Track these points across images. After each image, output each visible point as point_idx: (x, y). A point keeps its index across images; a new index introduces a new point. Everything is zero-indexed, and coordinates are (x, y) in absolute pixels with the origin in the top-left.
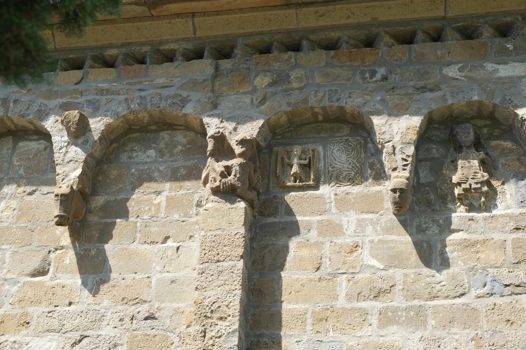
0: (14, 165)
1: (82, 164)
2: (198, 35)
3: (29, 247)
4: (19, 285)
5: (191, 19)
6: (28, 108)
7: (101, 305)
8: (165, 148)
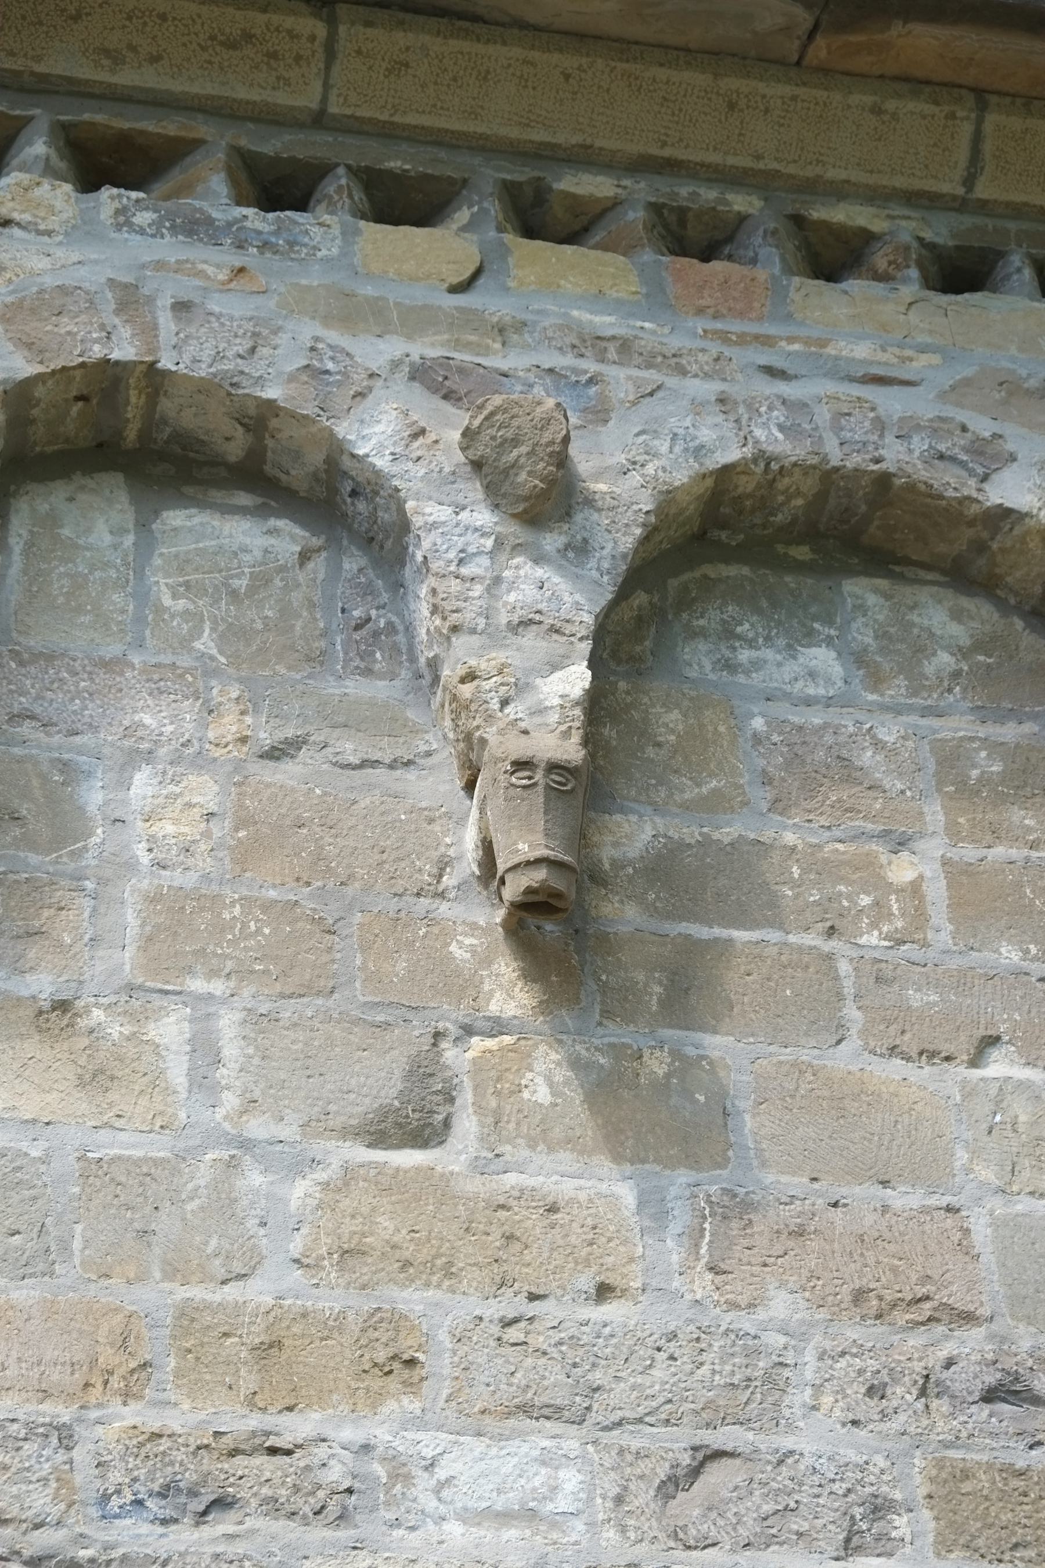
0: (159, 610)
1: (586, 647)
2: (983, 190)
3: (330, 1003)
4: (321, 1176)
5: (973, 115)
6: (253, 350)
7: (761, 1315)
8: (882, 651)
